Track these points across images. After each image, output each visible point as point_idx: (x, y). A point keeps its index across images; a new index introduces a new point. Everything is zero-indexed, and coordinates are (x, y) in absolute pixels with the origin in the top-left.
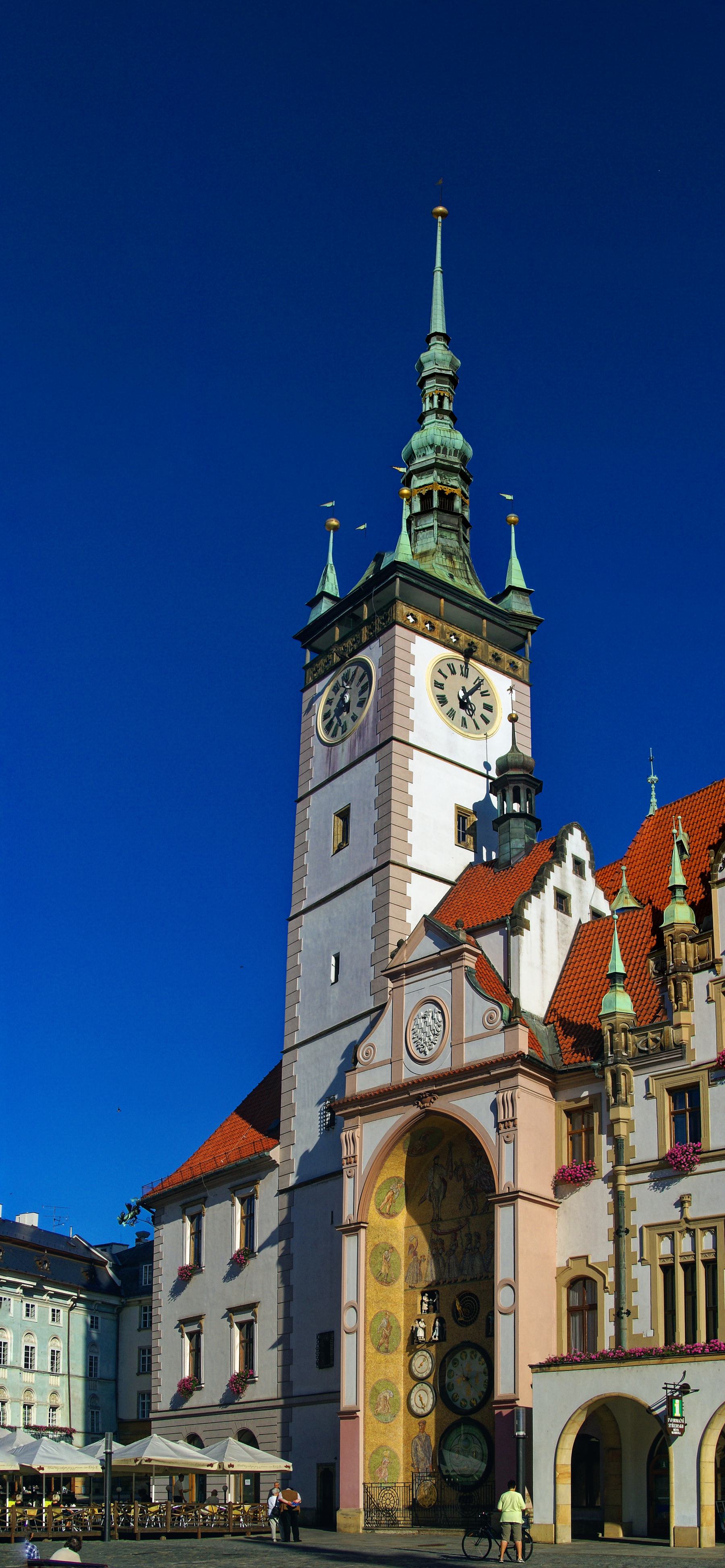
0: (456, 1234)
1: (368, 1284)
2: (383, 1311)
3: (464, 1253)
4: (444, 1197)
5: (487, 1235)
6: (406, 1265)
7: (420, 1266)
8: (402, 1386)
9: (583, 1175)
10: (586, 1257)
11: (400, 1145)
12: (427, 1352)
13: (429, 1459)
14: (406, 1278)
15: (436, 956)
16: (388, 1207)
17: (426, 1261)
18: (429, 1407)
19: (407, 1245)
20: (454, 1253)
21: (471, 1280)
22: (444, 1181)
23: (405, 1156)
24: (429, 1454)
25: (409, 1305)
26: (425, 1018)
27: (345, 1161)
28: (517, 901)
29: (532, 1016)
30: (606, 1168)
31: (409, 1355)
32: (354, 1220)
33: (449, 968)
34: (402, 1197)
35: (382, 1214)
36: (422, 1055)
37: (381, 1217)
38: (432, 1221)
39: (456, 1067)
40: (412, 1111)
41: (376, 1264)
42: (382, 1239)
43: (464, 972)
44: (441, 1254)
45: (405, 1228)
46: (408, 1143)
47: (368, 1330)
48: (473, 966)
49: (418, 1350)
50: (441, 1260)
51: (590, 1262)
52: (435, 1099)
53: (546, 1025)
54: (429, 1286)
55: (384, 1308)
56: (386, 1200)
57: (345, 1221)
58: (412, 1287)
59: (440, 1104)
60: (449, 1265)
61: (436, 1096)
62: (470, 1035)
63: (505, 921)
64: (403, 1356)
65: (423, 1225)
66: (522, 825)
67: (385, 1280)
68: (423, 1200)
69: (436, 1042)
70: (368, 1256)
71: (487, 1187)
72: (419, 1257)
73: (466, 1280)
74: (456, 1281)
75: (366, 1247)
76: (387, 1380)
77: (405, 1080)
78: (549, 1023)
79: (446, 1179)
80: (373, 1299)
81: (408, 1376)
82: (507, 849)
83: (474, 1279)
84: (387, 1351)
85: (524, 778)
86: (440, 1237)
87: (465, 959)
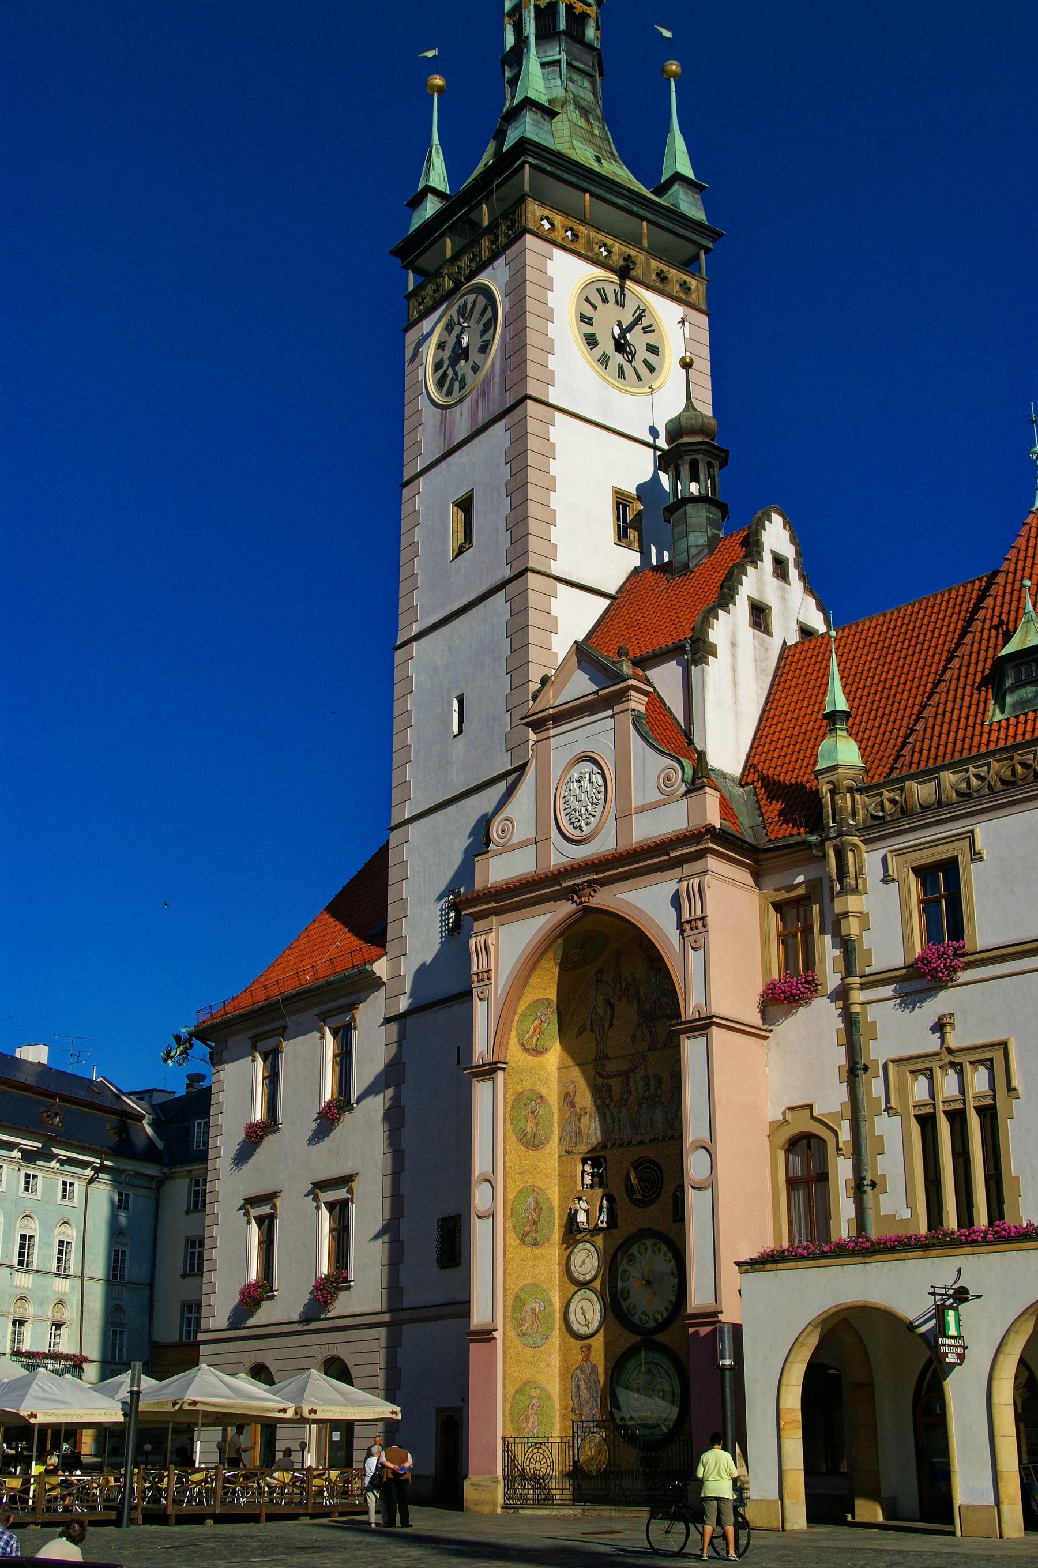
0: (628, 1078)
1: (508, 1147)
2: (530, 1186)
3: (640, 1104)
4: (611, 1025)
5: (671, 1078)
6: (560, 1121)
8: (557, 1293)
9: (801, 992)
10: (810, 1107)
11: (550, 954)
12: (592, 1244)
14: (560, 1140)
15: (592, 697)
16: (534, 1040)
17: (587, 1116)
18: (595, 1325)
19: (561, 1092)
21: (651, 1141)
22: (609, 1003)
23: (556, 970)
24: (597, 1394)
25: (565, 1178)
26: (579, 781)
28: (698, 618)
29: (724, 775)
30: (832, 981)
31: (566, 1249)
32: (488, 1059)
33: (610, 712)
34: (555, 1027)
35: (526, 1050)
36: (577, 832)
37: (525, 1055)
38: (595, 1060)
39: (623, 847)
40: (566, 908)
41: (520, 1120)
42: (527, 1085)
43: (630, 718)
44: (608, 1105)
45: (558, 1069)
46: (561, 952)
47: (509, 1212)
48: (642, 709)
49: (578, 1242)
51: (816, 1113)
52: (595, 891)
53: (743, 786)
54: (593, 1150)
55: (531, 1181)
56: (532, 1031)
57: (476, 1060)
58: (569, 1152)
59: (604, 898)
60: (620, 1121)
61: (597, 887)
62: (640, 803)
63: (684, 646)
64: (557, 1251)
65: (583, 1064)
66: (703, 513)
67: (532, 1143)
68: (582, 1030)
69: (595, 814)
70: (509, 1109)
71: (668, 1012)
72: (578, 1110)
73: (643, 1141)
74: (629, 1144)
75: (505, 1096)
76: (536, 1285)
77: (555, 865)
78: (747, 784)
79: (612, 1000)
80: (516, 1169)
81: (566, 1279)
82: (684, 546)
83: (654, 1139)
84: (535, 1243)
85: (703, 447)
87: (631, 700)
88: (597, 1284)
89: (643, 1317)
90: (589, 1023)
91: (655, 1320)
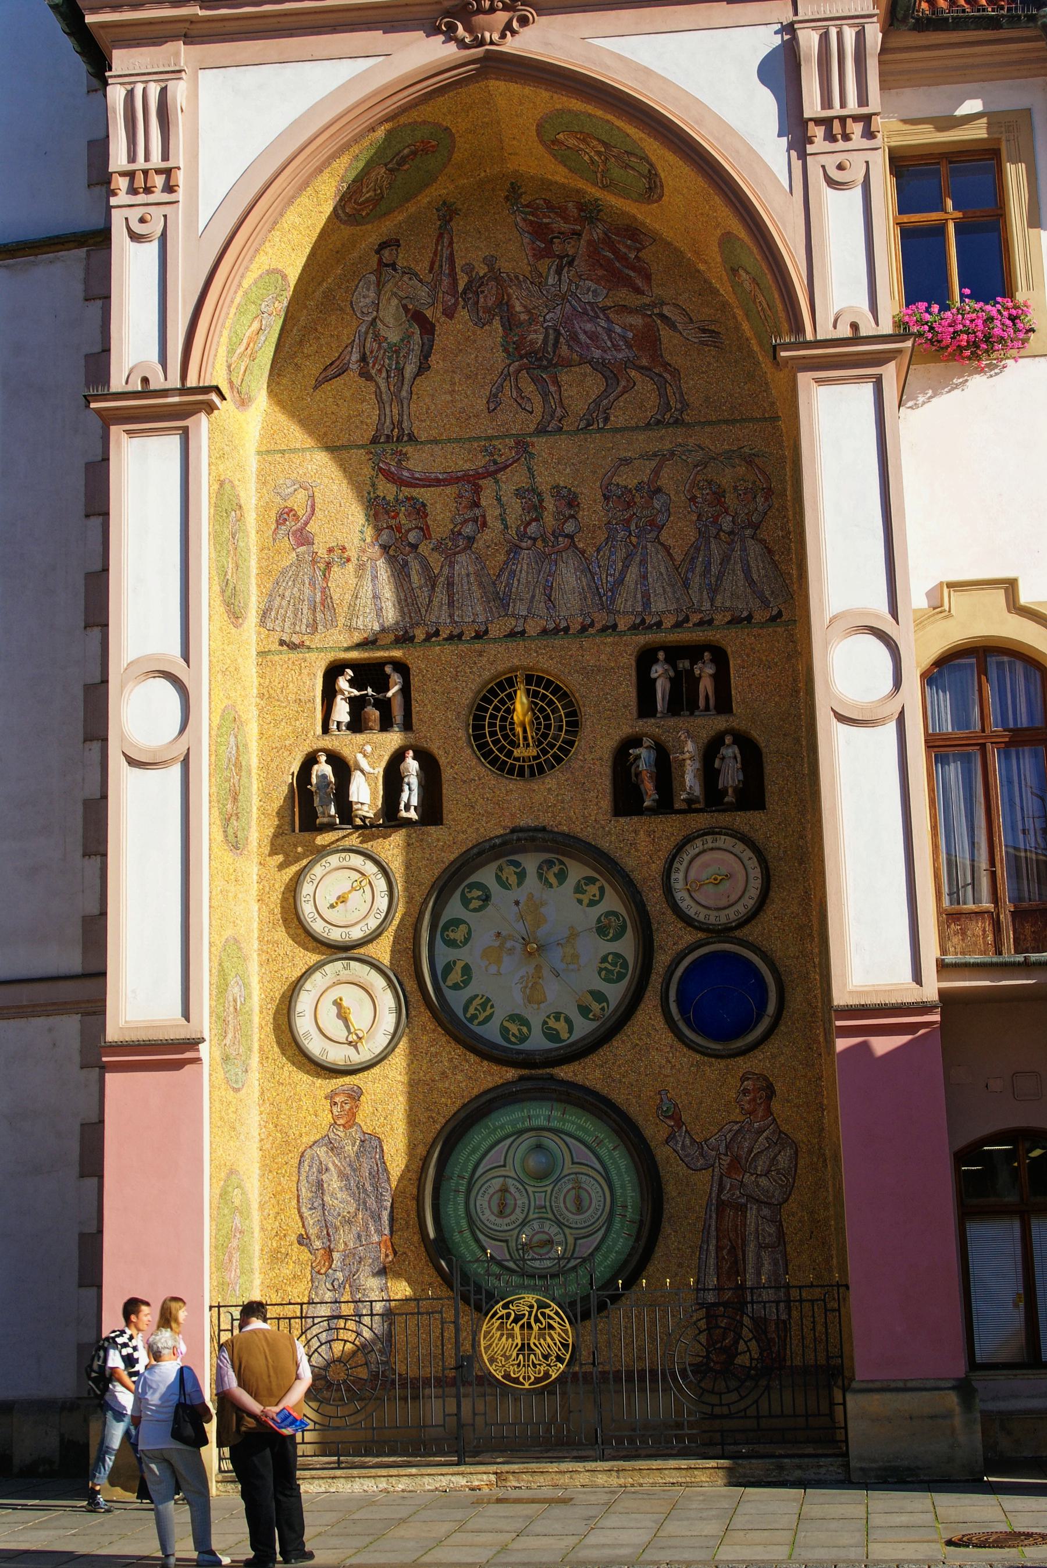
0: (477, 490)
3: (515, 549)
4: (423, 368)
5: (606, 498)
6: (264, 572)
7: (325, 577)
13: (377, 1218)
17: (351, 567)
18: (379, 1042)
19: (267, 508)
20: (468, 547)
21: (544, 632)
24: (379, 1199)
27: (122, 183)
31: (281, 867)
38: (374, 441)
44: (414, 547)
46: (361, 165)
49: (322, 852)
50: (415, 566)
51: (1025, 598)
52: (524, 21)
60: (450, 584)
65: (343, 447)
68: (334, 371)
71: (597, 353)
72: (322, 552)
73: (523, 633)
79: (428, 313)
83: (556, 631)
86: (407, 491)
88: (382, 950)
89: (514, 1028)
90: (355, 357)
91: (552, 1035)
